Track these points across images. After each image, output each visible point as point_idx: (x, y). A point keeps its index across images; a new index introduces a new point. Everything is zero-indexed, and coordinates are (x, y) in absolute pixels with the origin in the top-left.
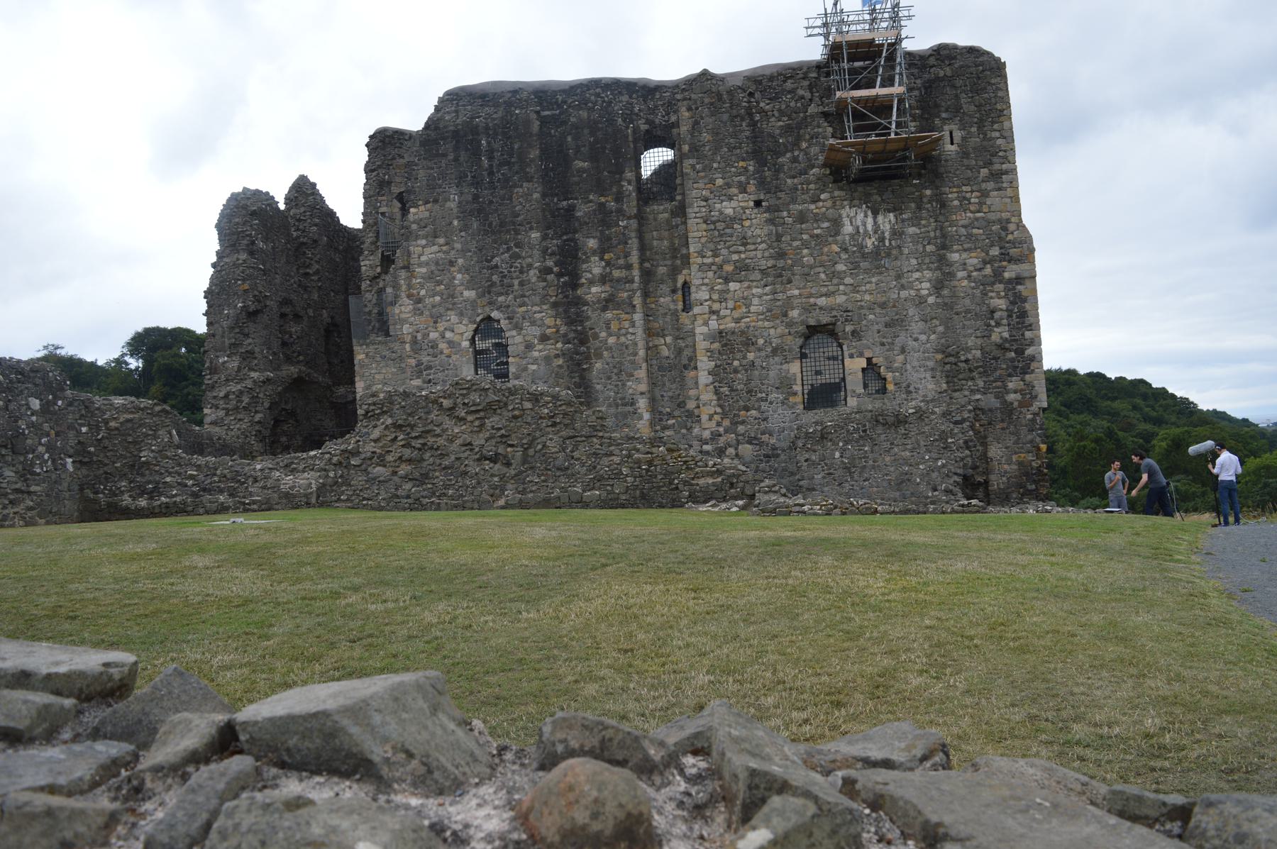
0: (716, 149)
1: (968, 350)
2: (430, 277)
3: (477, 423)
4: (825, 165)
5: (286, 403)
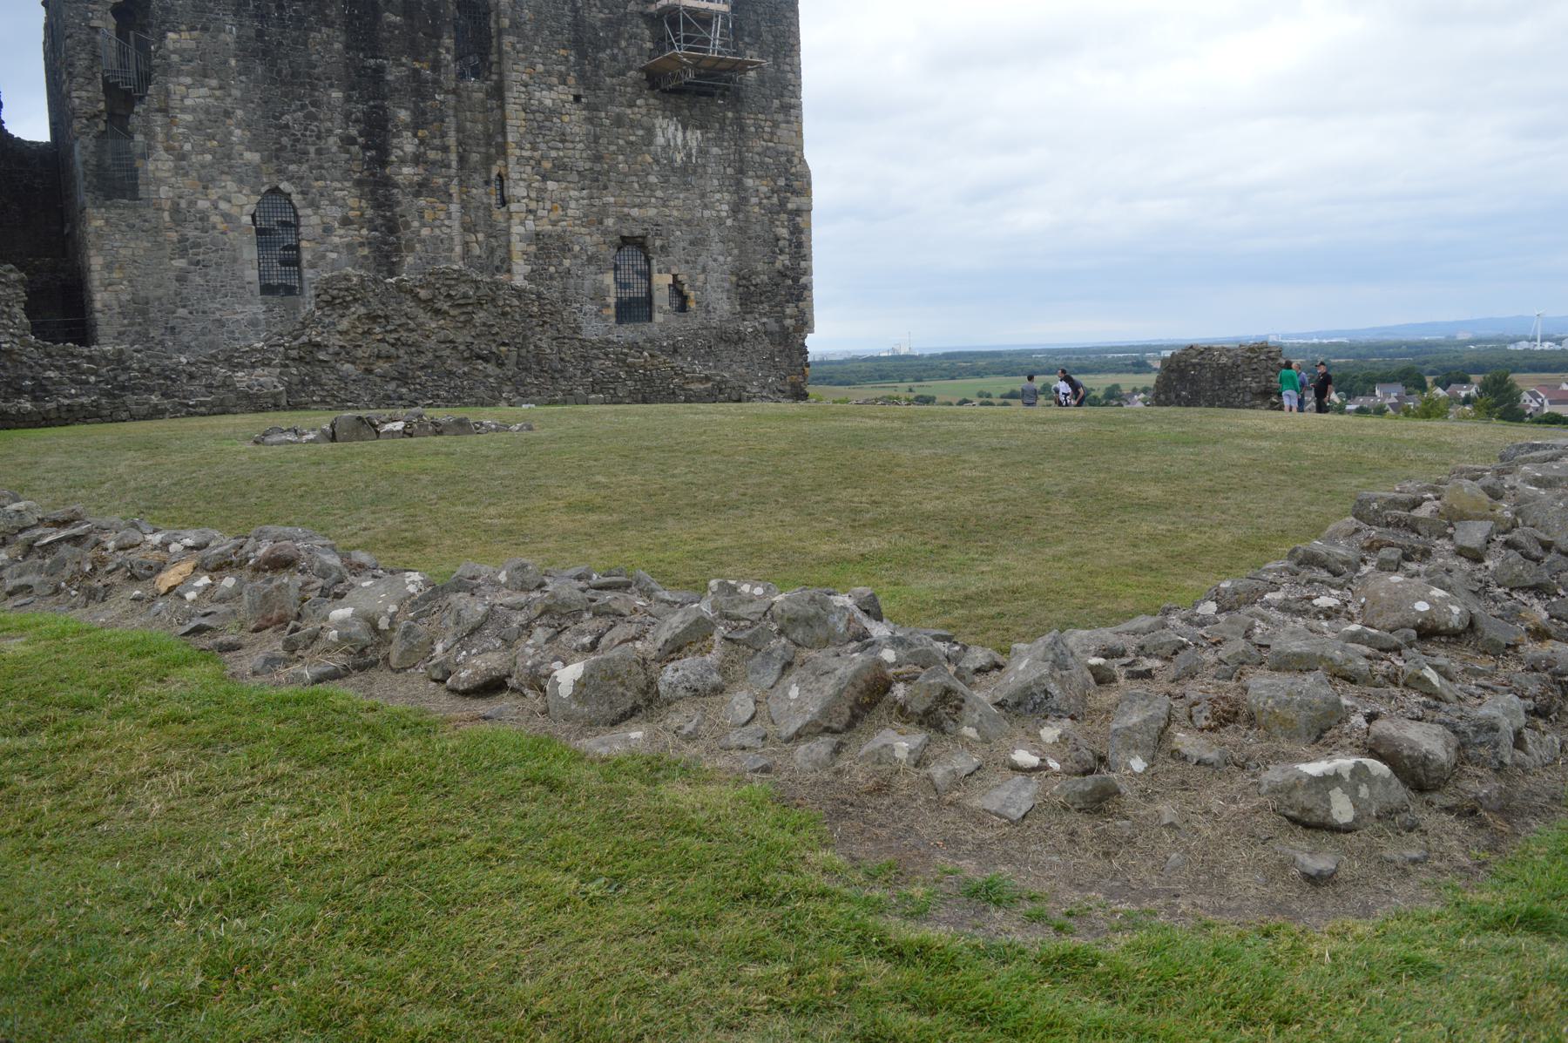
0: (538, 31)
1: (757, 274)
2: (198, 128)
3: (462, 318)
4: (642, 70)
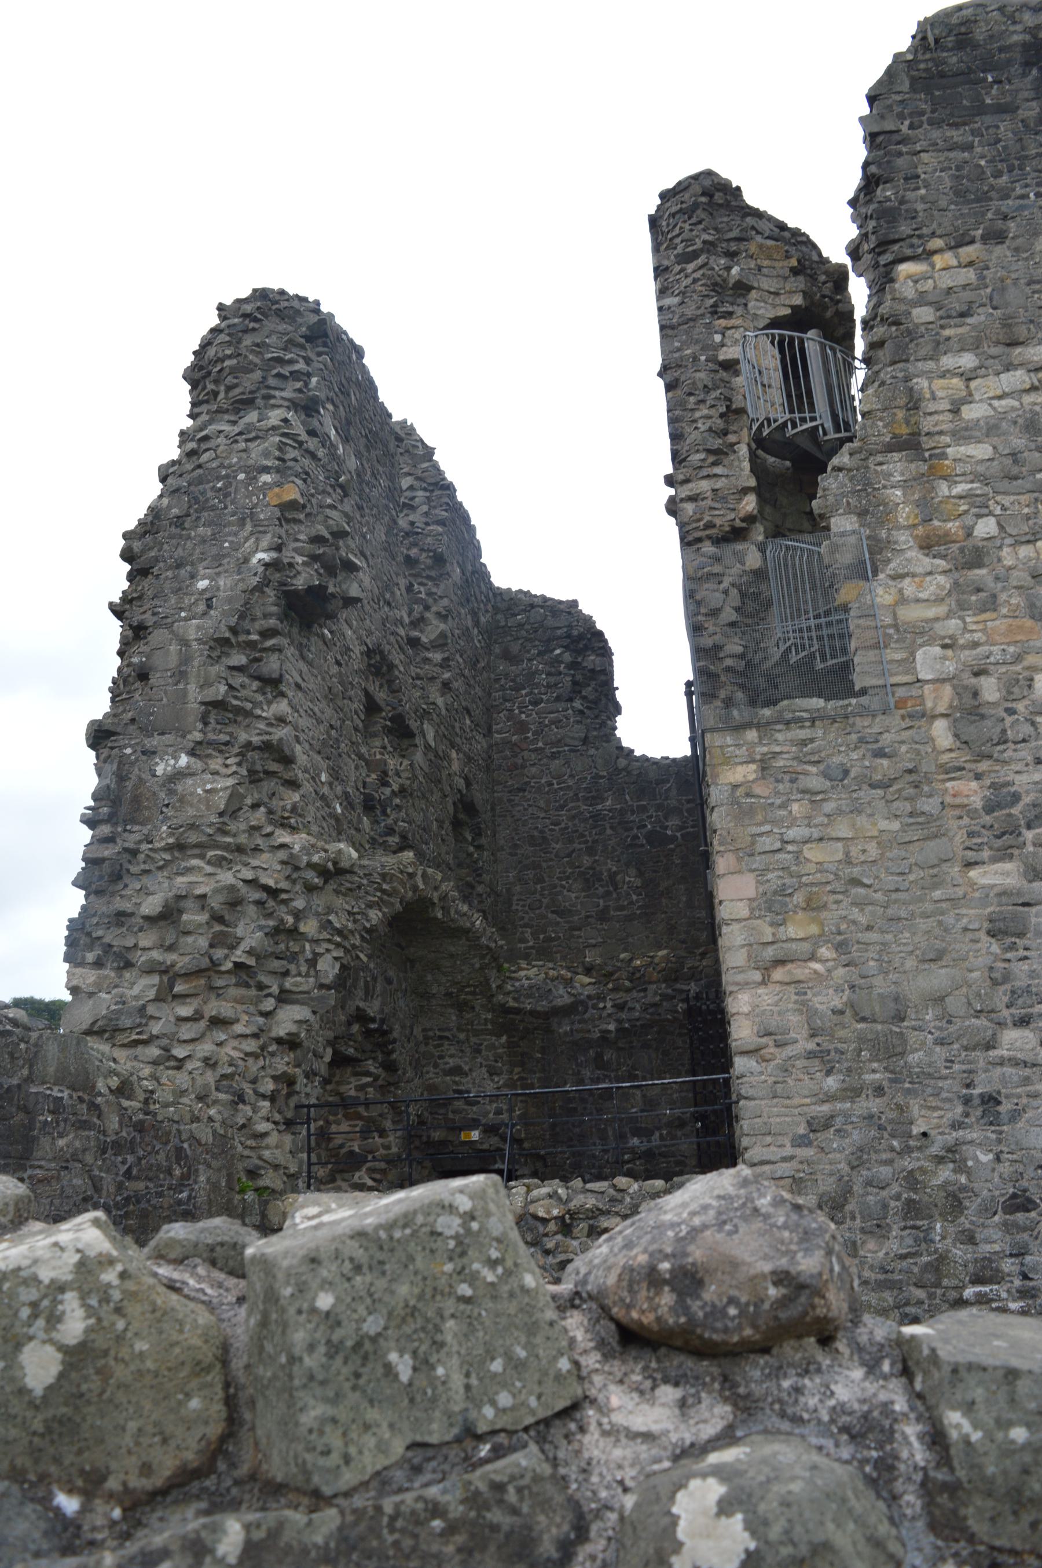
5: (368, 994)
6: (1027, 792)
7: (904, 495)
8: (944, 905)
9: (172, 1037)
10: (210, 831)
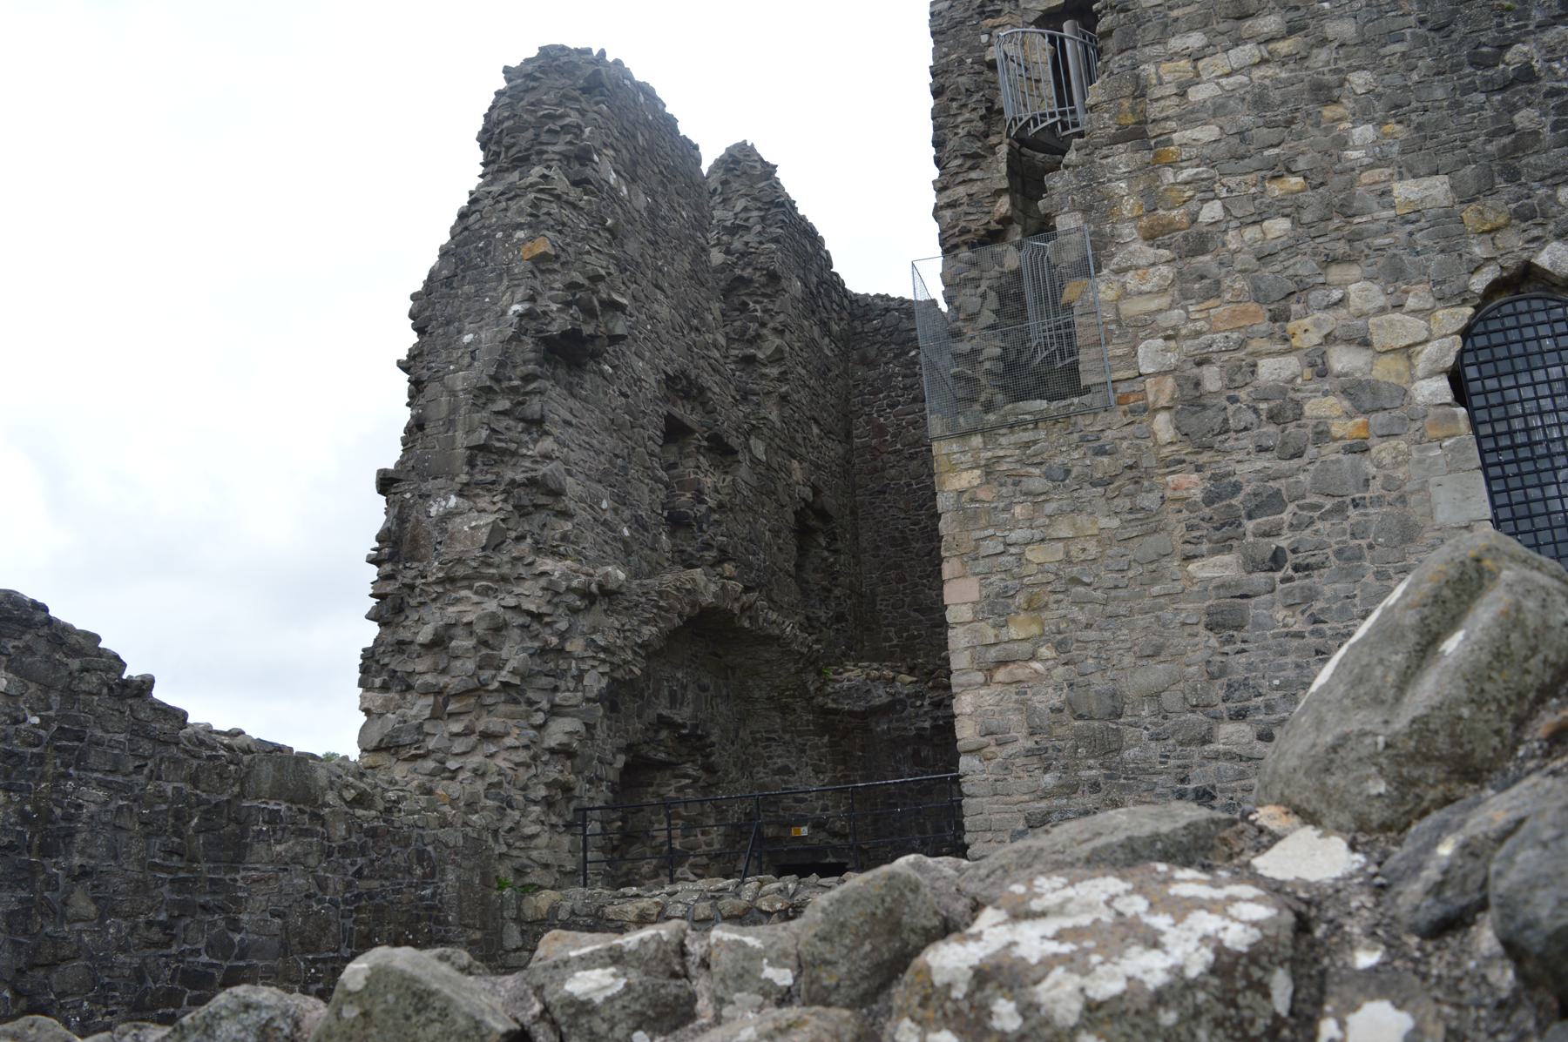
5: (674, 701)
6: (1249, 482)
7: (1129, 186)
8: (1162, 600)
9: (447, 751)
10: (474, 564)
